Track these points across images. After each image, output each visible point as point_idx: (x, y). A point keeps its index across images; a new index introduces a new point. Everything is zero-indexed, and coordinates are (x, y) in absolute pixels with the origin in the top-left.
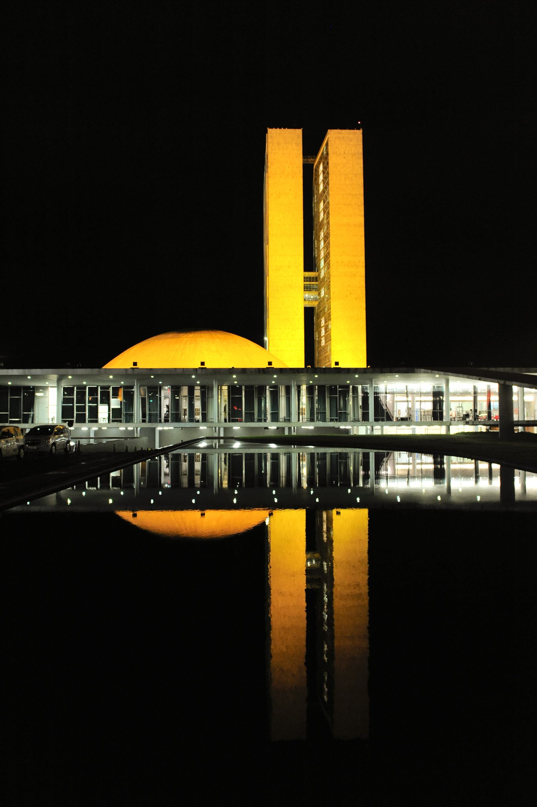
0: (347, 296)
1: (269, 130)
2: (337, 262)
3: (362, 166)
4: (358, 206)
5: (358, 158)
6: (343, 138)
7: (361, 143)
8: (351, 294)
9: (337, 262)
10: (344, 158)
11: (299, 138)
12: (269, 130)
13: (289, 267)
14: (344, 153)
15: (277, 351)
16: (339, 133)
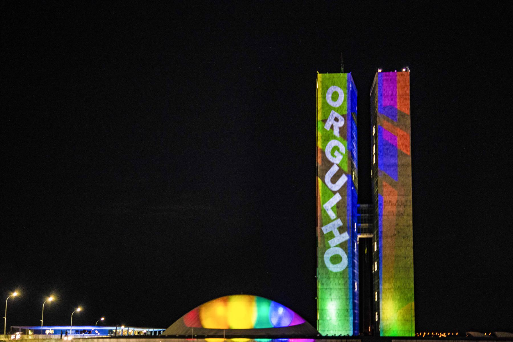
0: (395, 235)
3: (409, 107)
5: (406, 99)
6: (391, 80)
8: (398, 232)
15: (326, 289)
16: (386, 76)
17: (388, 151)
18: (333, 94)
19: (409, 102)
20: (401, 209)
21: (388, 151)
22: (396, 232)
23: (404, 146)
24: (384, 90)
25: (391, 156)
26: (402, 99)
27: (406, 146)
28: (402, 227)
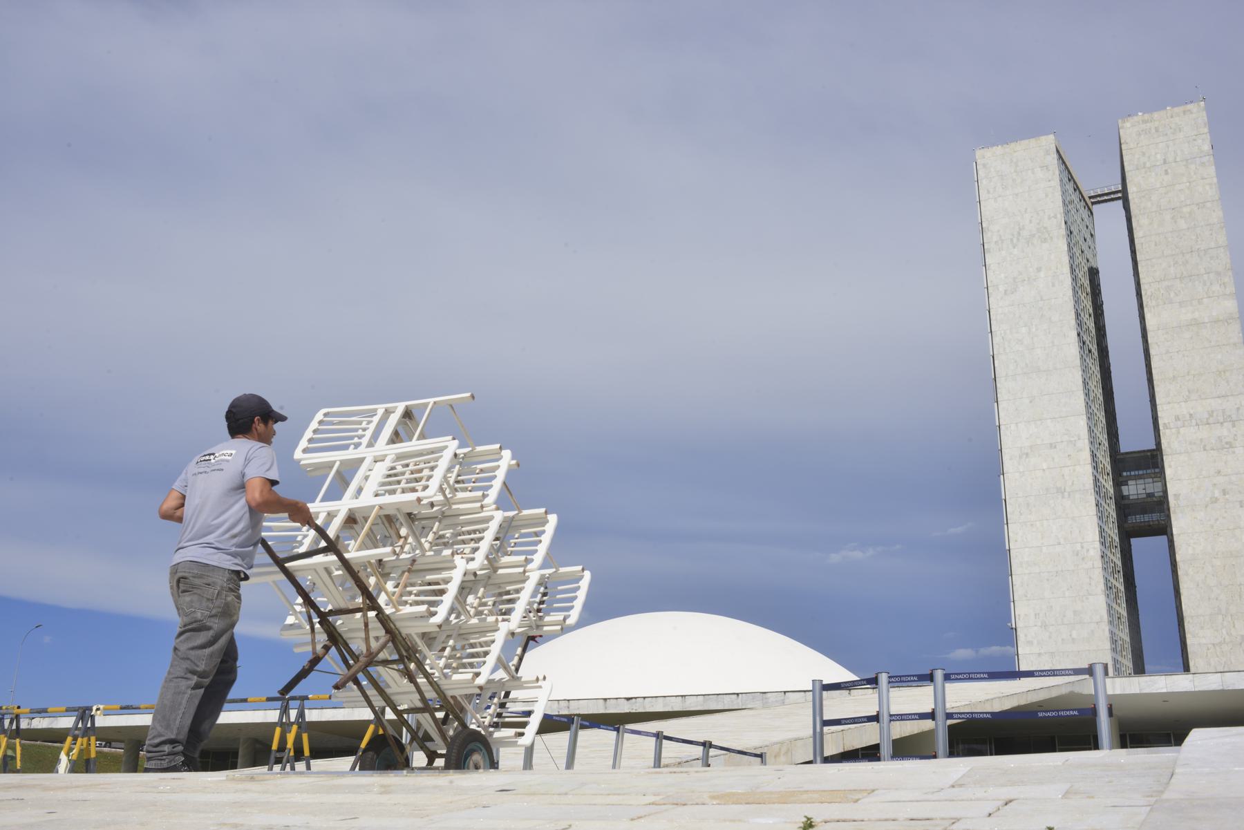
1: (979, 153)
2: (1177, 418)
3: (1215, 180)
4: (1218, 274)
5: (1203, 164)
6: (1157, 130)
7: (1206, 130)
8: (1224, 492)
9: (1177, 418)
10: (1166, 172)
11: (1047, 153)
12: (979, 153)
13: (1052, 446)
14: (1165, 162)
15: (1040, 654)
16: (1145, 122)
17: (1172, 295)
18: (1019, 188)
19: (1212, 170)
20: (1224, 431)
21: (1172, 295)
22: (1217, 494)
23: (1212, 275)
24: (1144, 154)
25: (1181, 304)
26: (1193, 167)
27: (1218, 274)
28: (1234, 478)
